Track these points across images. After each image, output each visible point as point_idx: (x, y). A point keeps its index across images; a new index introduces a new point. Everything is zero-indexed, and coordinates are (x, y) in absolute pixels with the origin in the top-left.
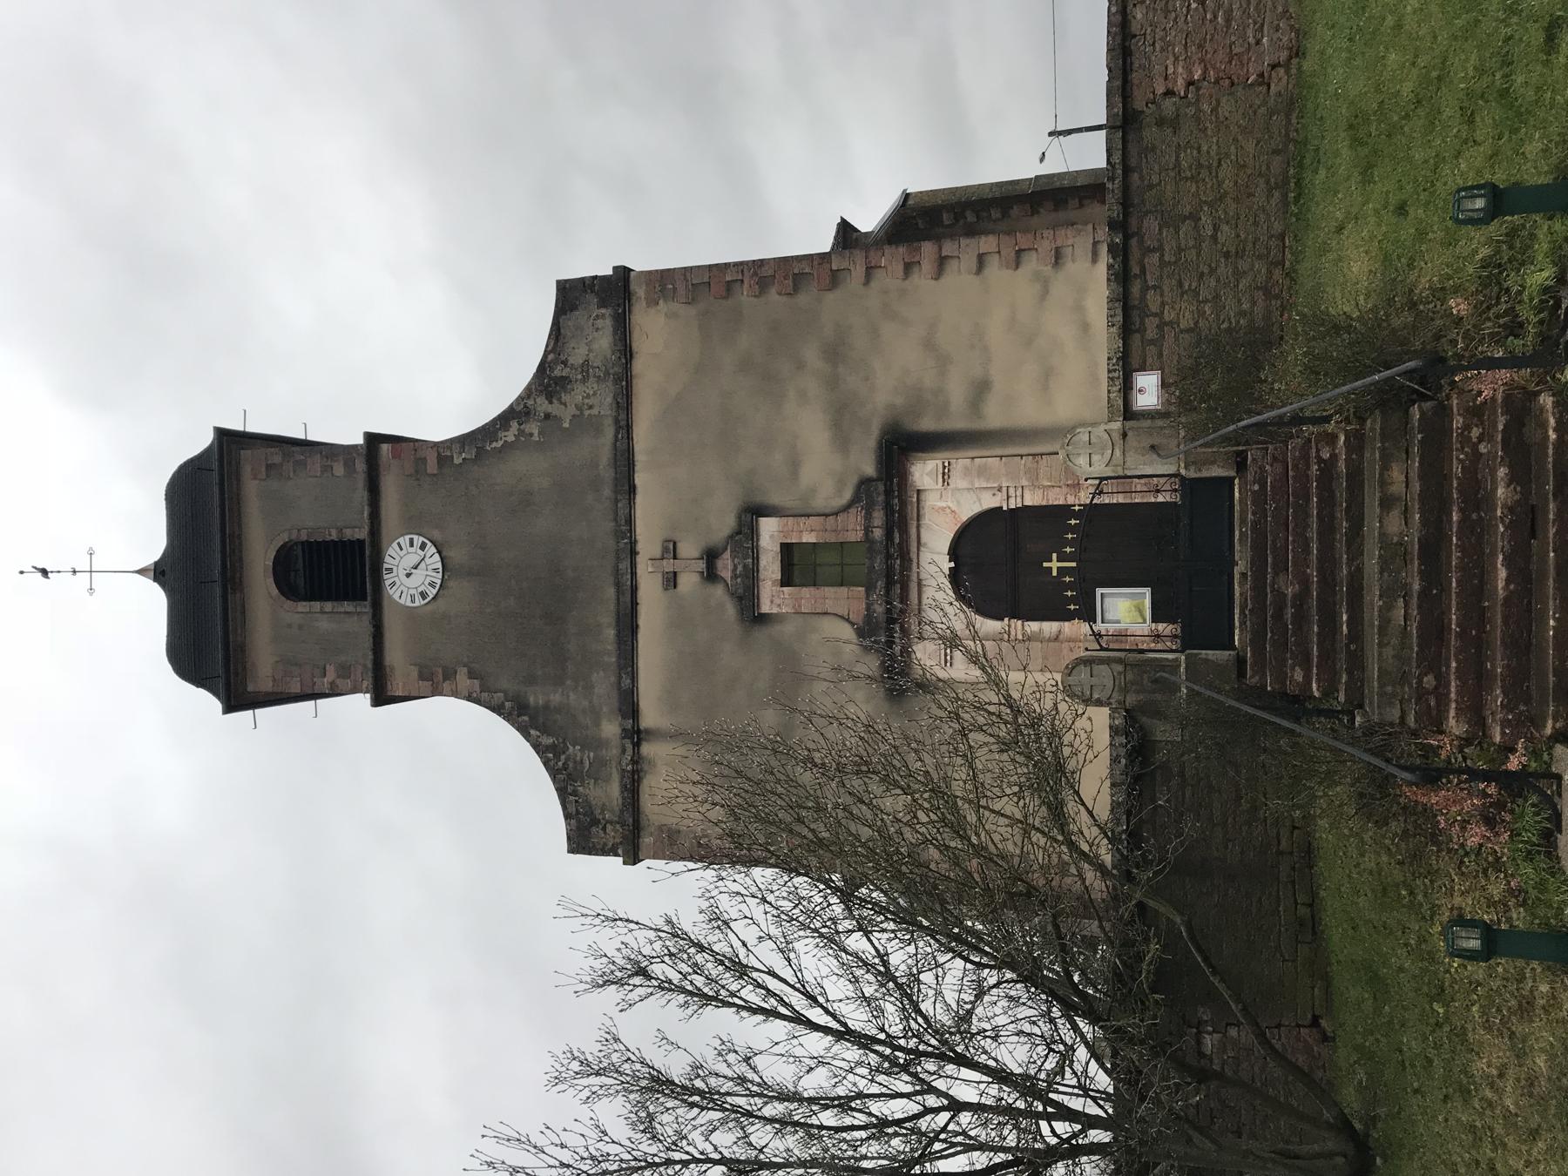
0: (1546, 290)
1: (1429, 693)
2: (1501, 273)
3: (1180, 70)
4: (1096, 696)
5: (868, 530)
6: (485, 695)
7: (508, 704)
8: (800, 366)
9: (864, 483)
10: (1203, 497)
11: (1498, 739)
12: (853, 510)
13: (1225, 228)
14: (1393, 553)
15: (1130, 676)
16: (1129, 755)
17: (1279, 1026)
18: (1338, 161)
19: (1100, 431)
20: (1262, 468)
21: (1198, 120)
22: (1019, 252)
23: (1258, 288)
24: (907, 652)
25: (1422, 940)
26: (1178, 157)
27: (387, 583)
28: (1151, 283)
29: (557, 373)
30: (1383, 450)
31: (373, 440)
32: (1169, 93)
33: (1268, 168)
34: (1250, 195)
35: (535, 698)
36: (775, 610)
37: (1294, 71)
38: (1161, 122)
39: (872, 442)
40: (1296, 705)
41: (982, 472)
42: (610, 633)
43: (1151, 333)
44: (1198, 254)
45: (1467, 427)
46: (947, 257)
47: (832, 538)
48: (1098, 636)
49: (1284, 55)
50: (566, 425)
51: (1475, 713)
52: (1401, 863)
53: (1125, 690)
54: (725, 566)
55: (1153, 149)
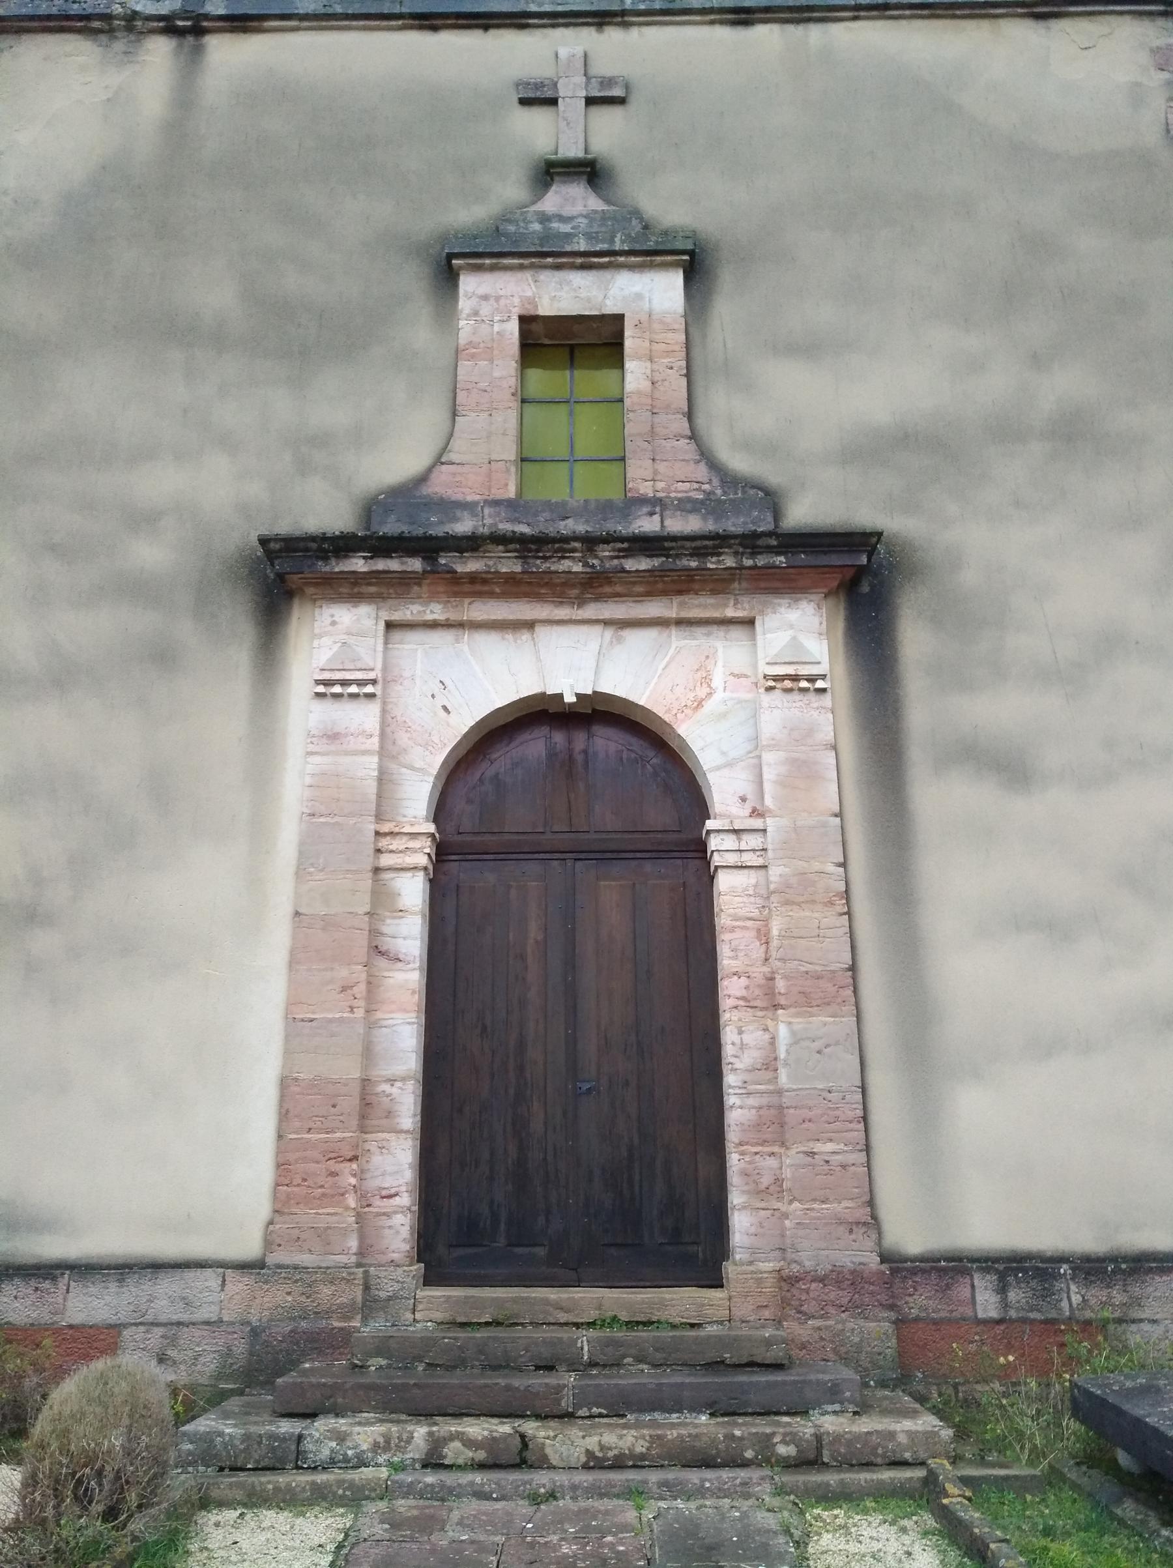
5: (657, 504)
8: (1037, 361)
9: (772, 500)
12: (701, 472)
24: (353, 589)
36: (465, 304)
39: (865, 517)
41: (801, 772)
47: (636, 424)
54: (571, 201)
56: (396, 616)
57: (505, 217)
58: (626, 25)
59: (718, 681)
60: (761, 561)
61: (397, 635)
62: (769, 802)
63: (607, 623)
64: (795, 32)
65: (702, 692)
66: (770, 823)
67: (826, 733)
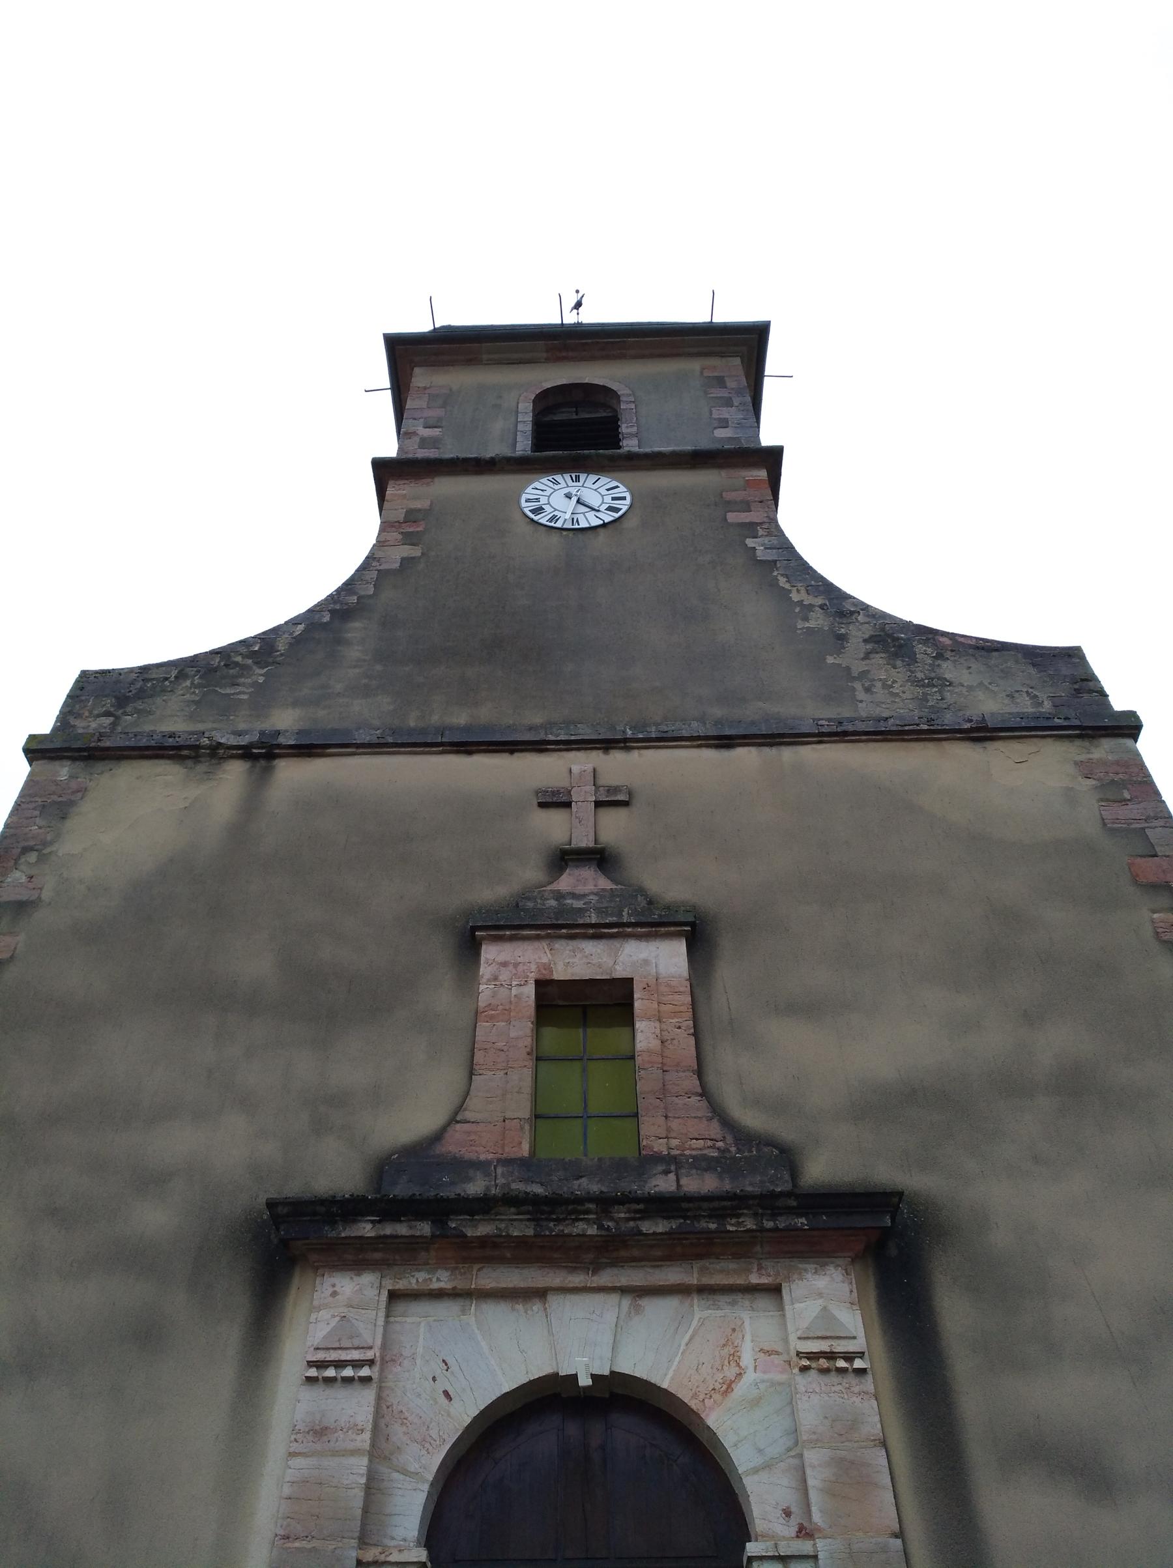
5: (671, 1162)
6: (374, 575)
7: (354, 599)
9: (787, 1157)
12: (715, 1129)
27: (558, 478)
29: (920, 648)
31: (772, 458)
35: (356, 629)
36: (485, 970)
39: (886, 1173)
41: (849, 1479)
42: (460, 718)
47: (647, 1082)
50: (830, 660)
54: (583, 882)
56: (401, 1285)
57: (525, 894)
58: (628, 749)
59: (747, 1359)
60: (782, 1223)
61: (400, 1307)
62: (817, 1517)
63: (624, 1291)
64: (770, 752)
65: (731, 1372)
66: (822, 1546)
67: (872, 1426)
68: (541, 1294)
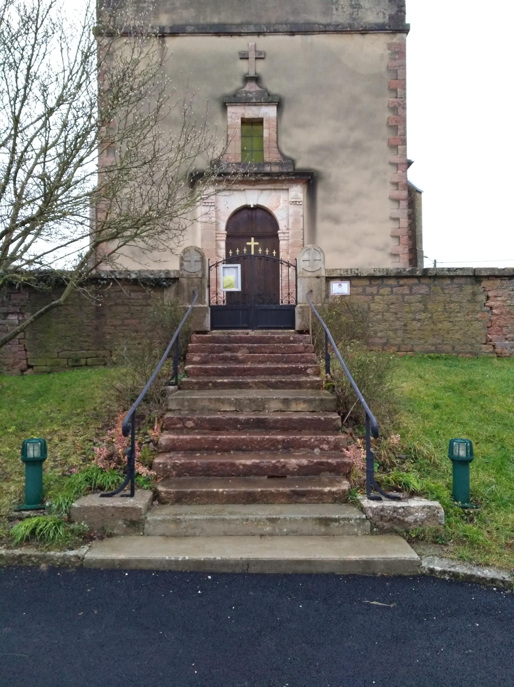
0: (407, 485)
1: (183, 424)
2: (412, 459)
3: (498, 303)
4: (185, 263)
5: (270, 164)
8: (352, 129)
9: (293, 162)
10: (286, 316)
11: (157, 461)
12: (279, 156)
13: (419, 324)
14: (260, 405)
15: (196, 280)
16: (156, 279)
17: (26, 350)
18: (453, 376)
19: (320, 265)
20: (301, 341)
21: (473, 312)
22: (399, 237)
23: (388, 340)
25: (52, 420)
26: (456, 302)
28: (394, 289)
30: (315, 400)
32: (488, 298)
33: (447, 344)
34: (434, 336)
36: (229, 115)
37: (491, 355)
38: (474, 294)
40: (180, 356)
41: (296, 221)
43: (369, 290)
44: (407, 312)
45: (328, 443)
46: (399, 203)
47: (265, 145)
48: (216, 265)
49: (498, 350)
51: (172, 448)
52: (95, 409)
53: (189, 278)
54: (252, 87)
55: (461, 291)
57: (237, 91)
58: (265, 35)
59: (281, 202)
60: (290, 178)
62: (290, 227)
63: (259, 189)
64: (304, 37)
66: (290, 231)
67: (301, 213)
68: (244, 190)
